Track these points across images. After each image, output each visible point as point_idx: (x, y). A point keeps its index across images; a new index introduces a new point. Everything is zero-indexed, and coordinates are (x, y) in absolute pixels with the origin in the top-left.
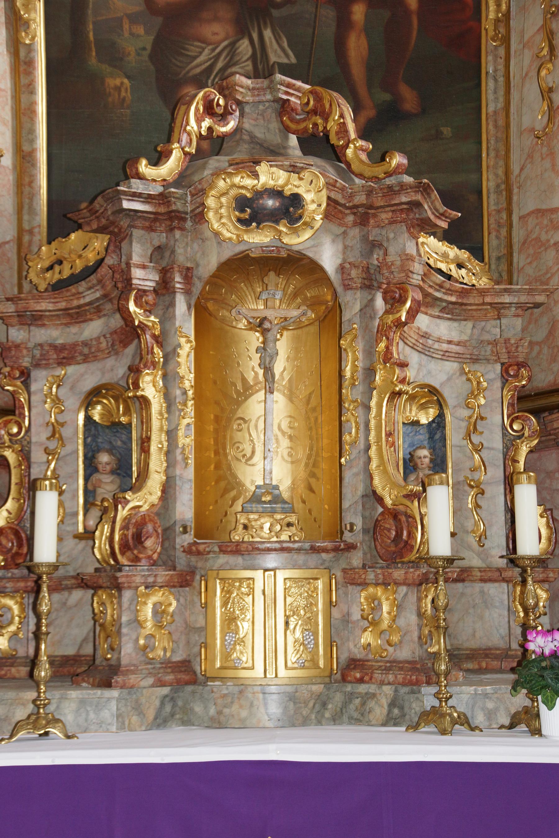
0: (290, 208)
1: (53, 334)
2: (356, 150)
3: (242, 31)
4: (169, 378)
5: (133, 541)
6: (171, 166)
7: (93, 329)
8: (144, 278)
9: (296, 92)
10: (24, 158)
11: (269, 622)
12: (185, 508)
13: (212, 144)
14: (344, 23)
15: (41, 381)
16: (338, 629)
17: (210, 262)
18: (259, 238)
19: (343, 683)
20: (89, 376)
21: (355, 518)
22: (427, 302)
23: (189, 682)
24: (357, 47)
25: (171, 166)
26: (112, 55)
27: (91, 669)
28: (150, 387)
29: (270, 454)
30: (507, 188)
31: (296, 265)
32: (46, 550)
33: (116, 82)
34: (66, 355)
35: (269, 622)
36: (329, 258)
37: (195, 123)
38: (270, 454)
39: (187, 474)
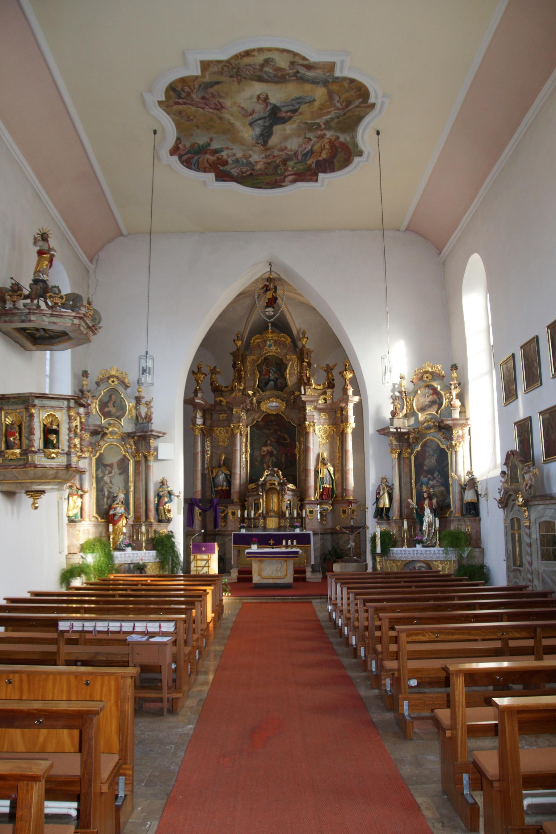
0: (274, 484)
1: (251, 493)
2: (282, 477)
3: (271, 457)
4: (263, 500)
5: (260, 515)
6: (263, 478)
7: (255, 493)
8: (260, 490)
9: (275, 469)
10: (247, 472)
11: (272, 523)
12: (264, 512)
13: (267, 475)
14: (282, 456)
15: (250, 498)
16: (279, 523)
17: (267, 488)
18: (271, 487)
19: (279, 528)
20: (255, 498)
21: (281, 513)
22: (288, 490)
23: (265, 528)
24: (283, 459)
25: (263, 478)
26: (256, 460)
27: (256, 527)
28: (261, 501)
29: (274, 505)
30: (299, 476)
31: (275, 489)
32: (252, 516)
33: (257, 463)
34: (252, 495)
35: (272, 523)
36: (278, 488)
37: (266, 474)
38: (274, 505)
39: (265, 509)
